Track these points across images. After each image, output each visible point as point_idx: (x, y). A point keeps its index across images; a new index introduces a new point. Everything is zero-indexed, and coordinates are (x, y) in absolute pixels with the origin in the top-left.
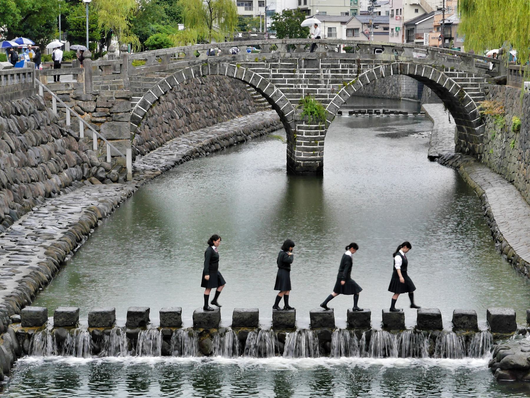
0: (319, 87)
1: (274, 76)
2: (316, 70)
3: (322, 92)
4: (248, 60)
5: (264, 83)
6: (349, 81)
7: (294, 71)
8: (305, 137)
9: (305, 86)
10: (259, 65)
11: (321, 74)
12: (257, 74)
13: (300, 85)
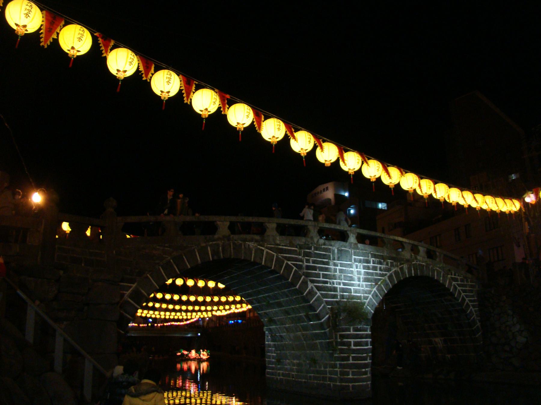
0: (352, 285)
1: (308, 268)
2: (349, 264)
3: (356, 291)
4: (278, 242)
5: (297, 277)
6: (380, 280)
7: (327, 263)
8: (354, 349)
9: (340, 284)
10: (289, 252)
11: (354, 269)
12: (289, 263)
13: (335, 281)
